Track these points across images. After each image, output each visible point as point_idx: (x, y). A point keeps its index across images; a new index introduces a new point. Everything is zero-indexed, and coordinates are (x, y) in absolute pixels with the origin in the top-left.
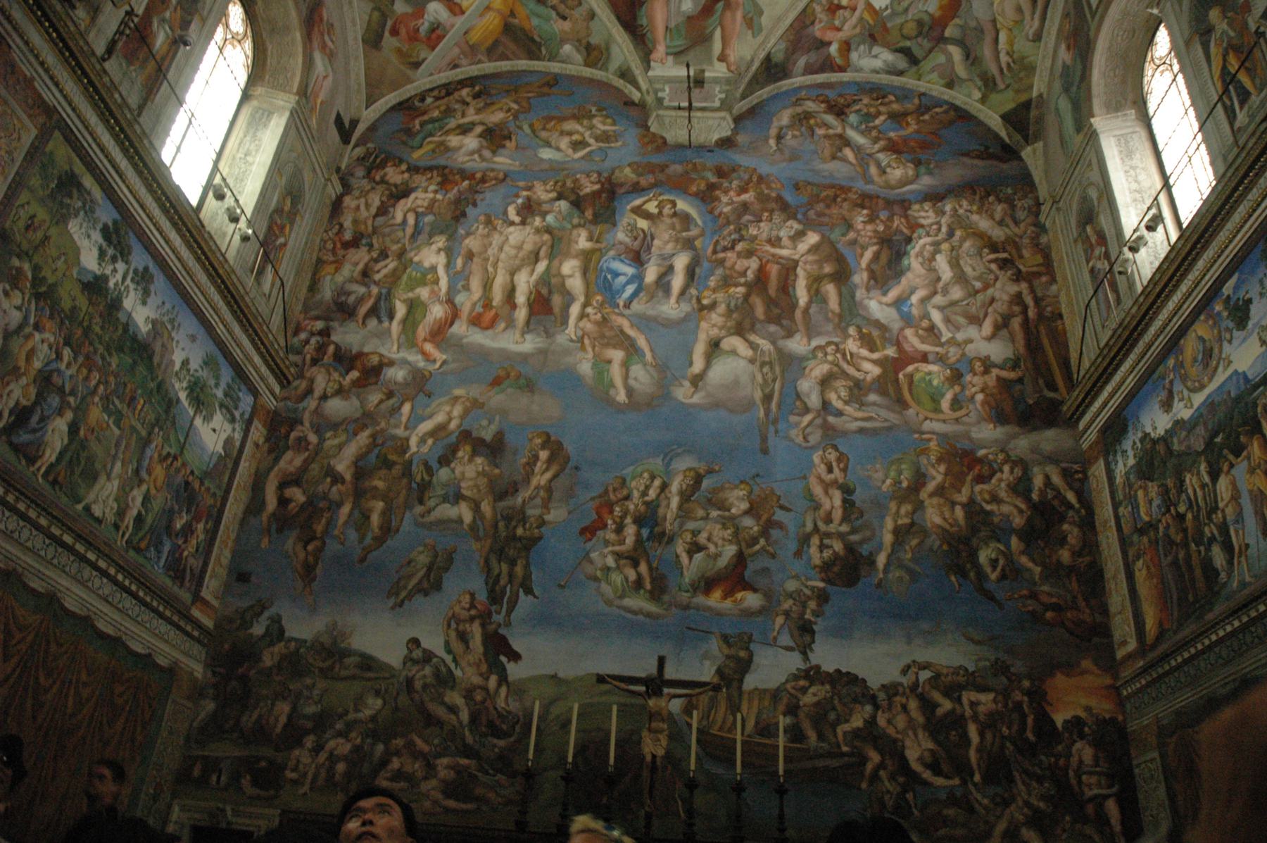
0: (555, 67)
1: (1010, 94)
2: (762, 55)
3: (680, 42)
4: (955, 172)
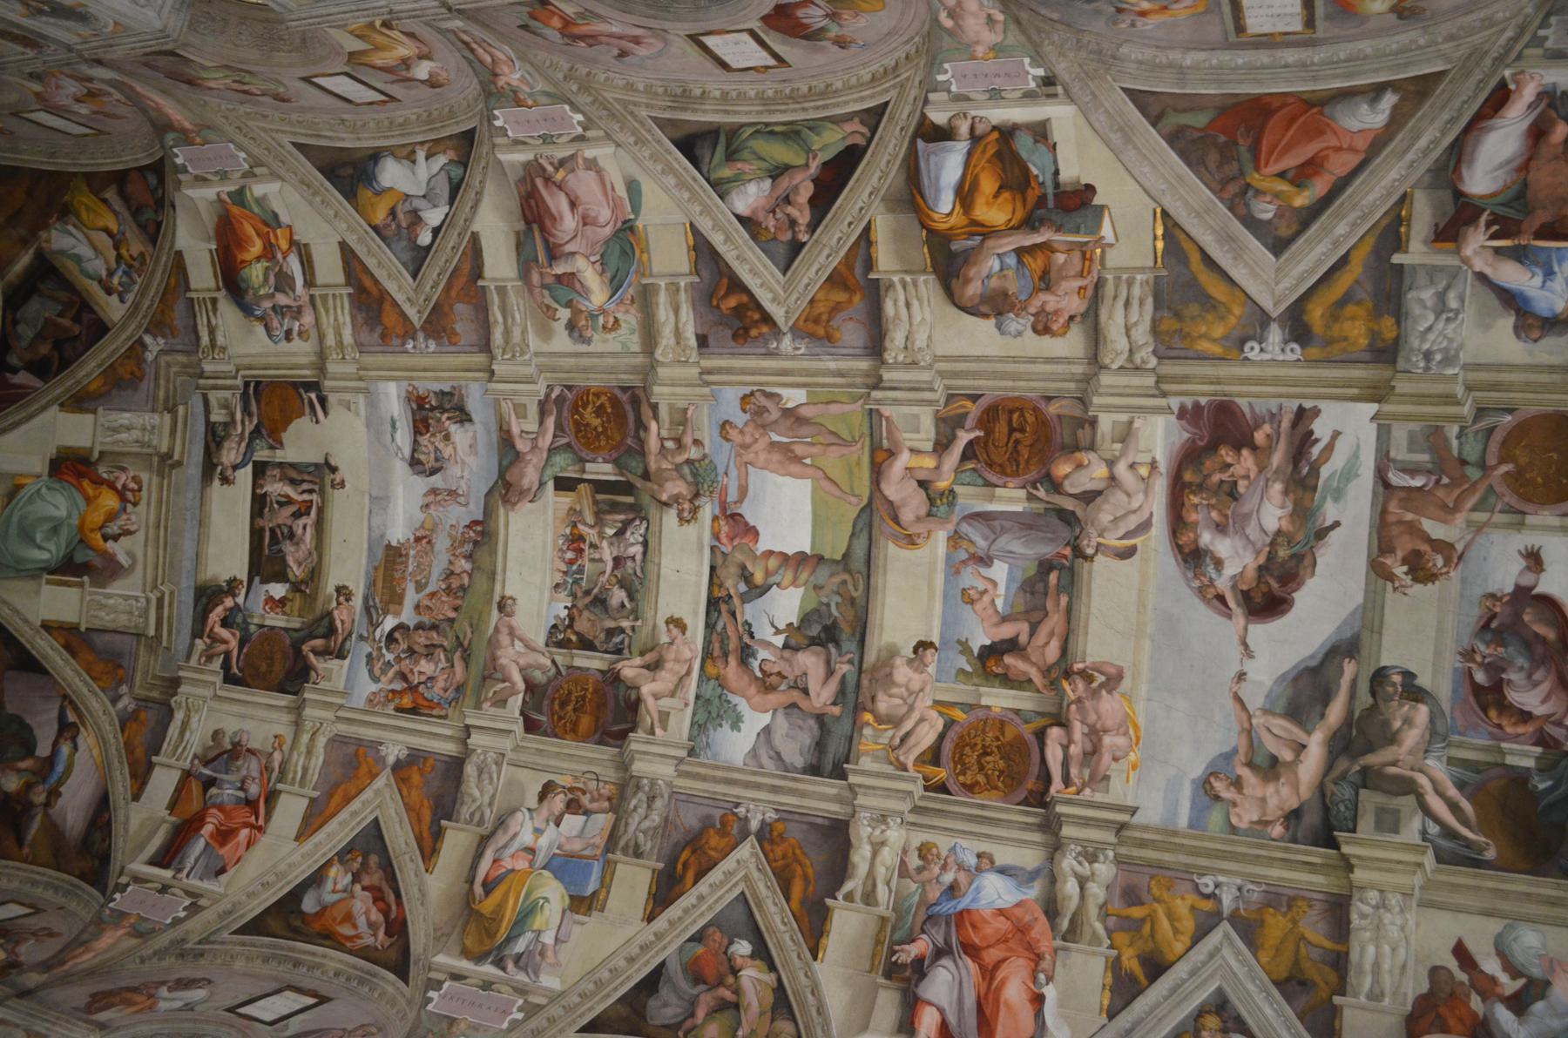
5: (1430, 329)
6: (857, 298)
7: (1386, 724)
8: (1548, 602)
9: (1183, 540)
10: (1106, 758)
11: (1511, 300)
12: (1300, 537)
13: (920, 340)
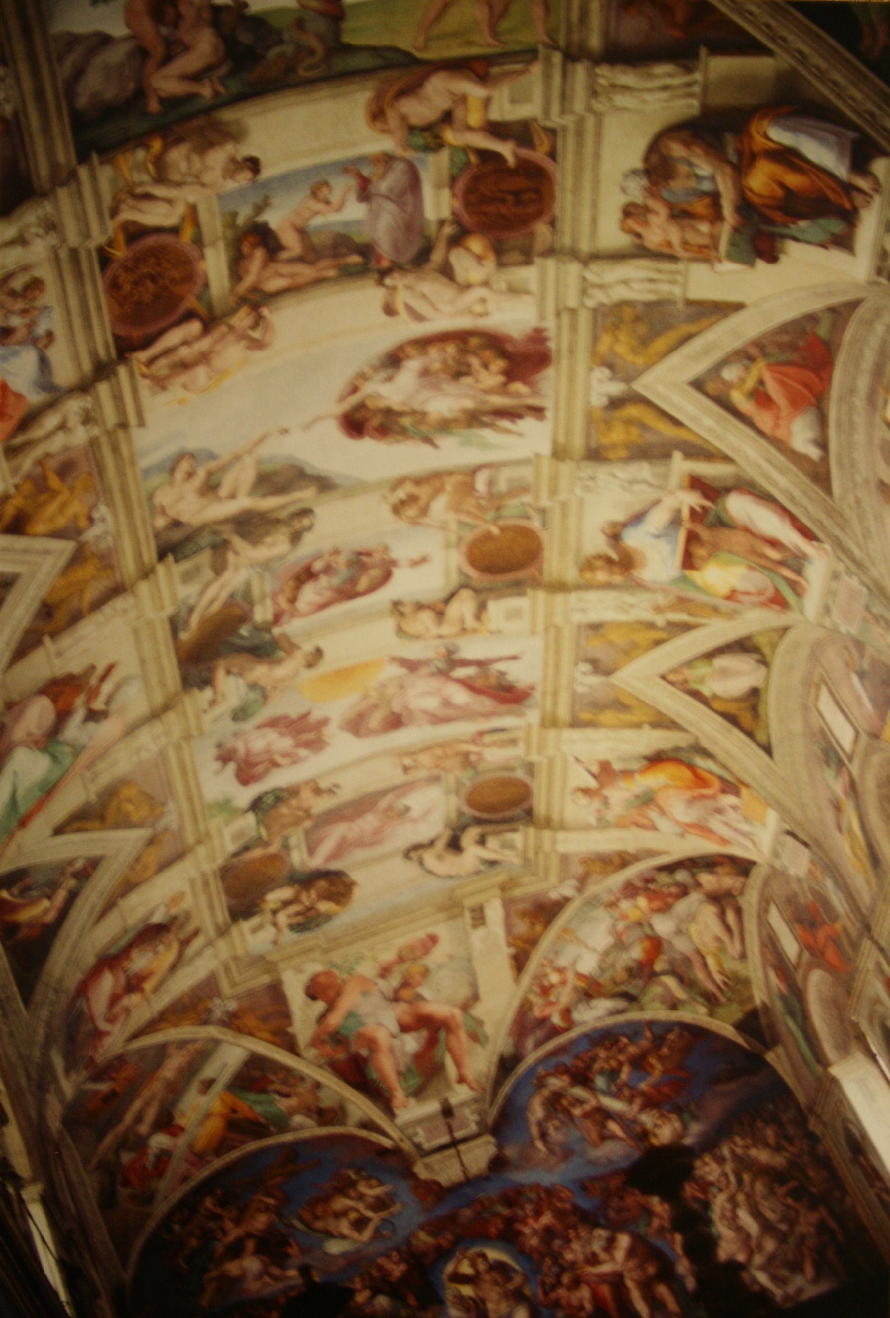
0: (288, 1137)
1: (734, 1007)
2: (495, 1059)
3: (414, 1082)
4: (716, 1107)
5: (614, 476)
6: (677, 33)
7: (268, 533)
8: (387, 576)
9: (410, 350)
10: (184, 378)
11: (638, 518)
12: (424, 428)
13: (620, 100)
